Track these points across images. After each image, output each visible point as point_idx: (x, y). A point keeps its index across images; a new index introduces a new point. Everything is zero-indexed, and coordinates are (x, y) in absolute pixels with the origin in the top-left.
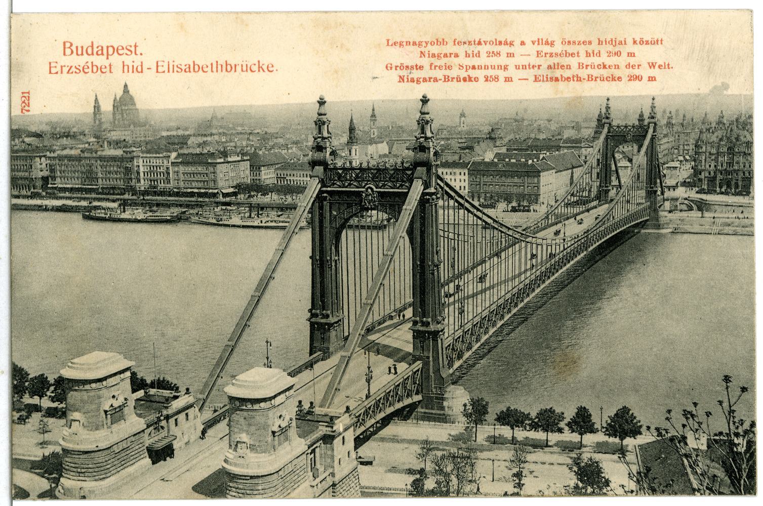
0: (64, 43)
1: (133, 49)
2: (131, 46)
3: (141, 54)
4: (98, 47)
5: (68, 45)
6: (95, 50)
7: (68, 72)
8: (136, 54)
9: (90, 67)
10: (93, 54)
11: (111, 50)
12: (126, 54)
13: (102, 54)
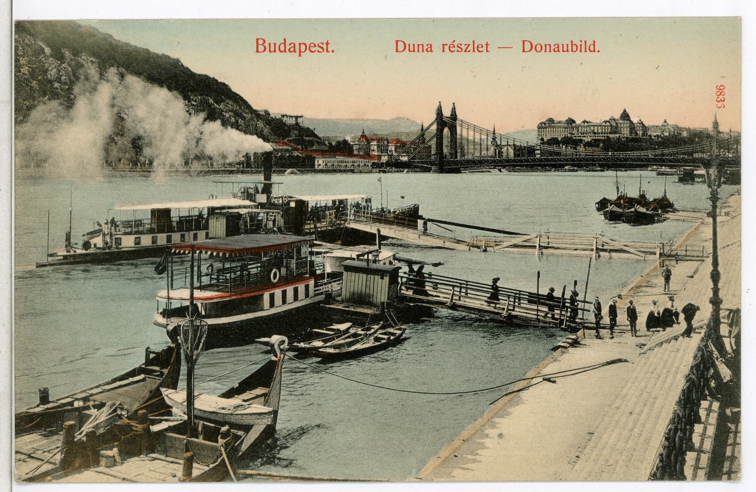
0: (257, 40)
1: (325, 46)
2: (323, 44)
3: (333, 51)
4: (290, 44)
5: (261, 42)
6: (288, 47)
8: (327, 51)
10: (285, 51)
12: (318, 51)
13: (295, 51)
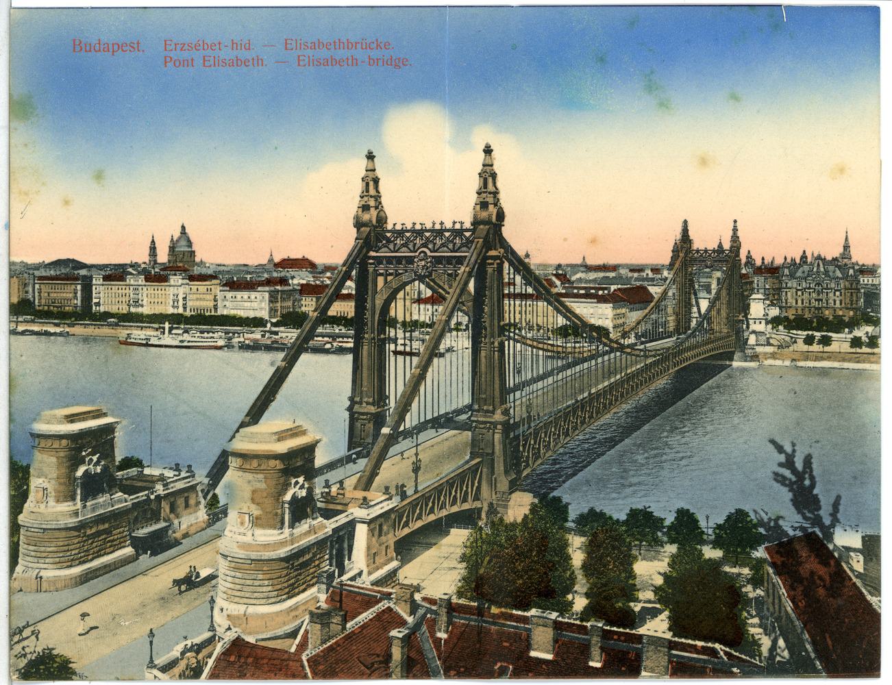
1: (136, 46)
6: (102, 47)
7: (181, 50)
8: (139, 51)
9: (202, 45)
10: (100, 51)
11: (116, 47)
